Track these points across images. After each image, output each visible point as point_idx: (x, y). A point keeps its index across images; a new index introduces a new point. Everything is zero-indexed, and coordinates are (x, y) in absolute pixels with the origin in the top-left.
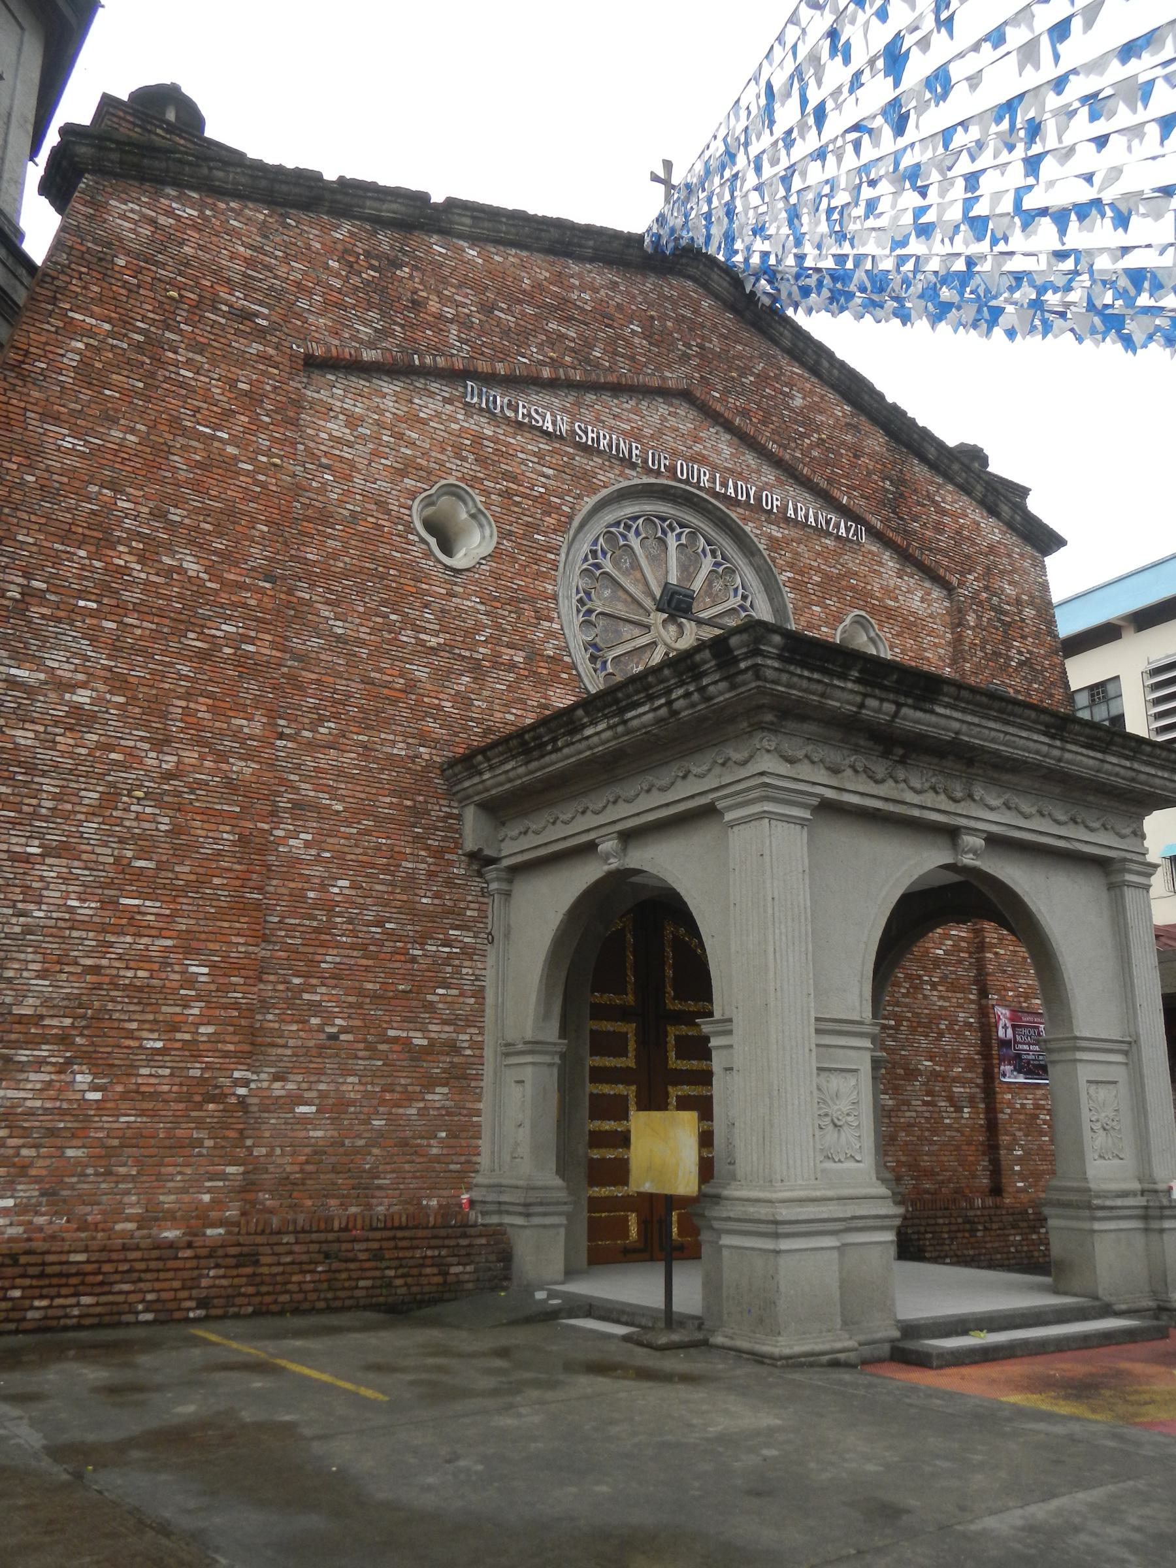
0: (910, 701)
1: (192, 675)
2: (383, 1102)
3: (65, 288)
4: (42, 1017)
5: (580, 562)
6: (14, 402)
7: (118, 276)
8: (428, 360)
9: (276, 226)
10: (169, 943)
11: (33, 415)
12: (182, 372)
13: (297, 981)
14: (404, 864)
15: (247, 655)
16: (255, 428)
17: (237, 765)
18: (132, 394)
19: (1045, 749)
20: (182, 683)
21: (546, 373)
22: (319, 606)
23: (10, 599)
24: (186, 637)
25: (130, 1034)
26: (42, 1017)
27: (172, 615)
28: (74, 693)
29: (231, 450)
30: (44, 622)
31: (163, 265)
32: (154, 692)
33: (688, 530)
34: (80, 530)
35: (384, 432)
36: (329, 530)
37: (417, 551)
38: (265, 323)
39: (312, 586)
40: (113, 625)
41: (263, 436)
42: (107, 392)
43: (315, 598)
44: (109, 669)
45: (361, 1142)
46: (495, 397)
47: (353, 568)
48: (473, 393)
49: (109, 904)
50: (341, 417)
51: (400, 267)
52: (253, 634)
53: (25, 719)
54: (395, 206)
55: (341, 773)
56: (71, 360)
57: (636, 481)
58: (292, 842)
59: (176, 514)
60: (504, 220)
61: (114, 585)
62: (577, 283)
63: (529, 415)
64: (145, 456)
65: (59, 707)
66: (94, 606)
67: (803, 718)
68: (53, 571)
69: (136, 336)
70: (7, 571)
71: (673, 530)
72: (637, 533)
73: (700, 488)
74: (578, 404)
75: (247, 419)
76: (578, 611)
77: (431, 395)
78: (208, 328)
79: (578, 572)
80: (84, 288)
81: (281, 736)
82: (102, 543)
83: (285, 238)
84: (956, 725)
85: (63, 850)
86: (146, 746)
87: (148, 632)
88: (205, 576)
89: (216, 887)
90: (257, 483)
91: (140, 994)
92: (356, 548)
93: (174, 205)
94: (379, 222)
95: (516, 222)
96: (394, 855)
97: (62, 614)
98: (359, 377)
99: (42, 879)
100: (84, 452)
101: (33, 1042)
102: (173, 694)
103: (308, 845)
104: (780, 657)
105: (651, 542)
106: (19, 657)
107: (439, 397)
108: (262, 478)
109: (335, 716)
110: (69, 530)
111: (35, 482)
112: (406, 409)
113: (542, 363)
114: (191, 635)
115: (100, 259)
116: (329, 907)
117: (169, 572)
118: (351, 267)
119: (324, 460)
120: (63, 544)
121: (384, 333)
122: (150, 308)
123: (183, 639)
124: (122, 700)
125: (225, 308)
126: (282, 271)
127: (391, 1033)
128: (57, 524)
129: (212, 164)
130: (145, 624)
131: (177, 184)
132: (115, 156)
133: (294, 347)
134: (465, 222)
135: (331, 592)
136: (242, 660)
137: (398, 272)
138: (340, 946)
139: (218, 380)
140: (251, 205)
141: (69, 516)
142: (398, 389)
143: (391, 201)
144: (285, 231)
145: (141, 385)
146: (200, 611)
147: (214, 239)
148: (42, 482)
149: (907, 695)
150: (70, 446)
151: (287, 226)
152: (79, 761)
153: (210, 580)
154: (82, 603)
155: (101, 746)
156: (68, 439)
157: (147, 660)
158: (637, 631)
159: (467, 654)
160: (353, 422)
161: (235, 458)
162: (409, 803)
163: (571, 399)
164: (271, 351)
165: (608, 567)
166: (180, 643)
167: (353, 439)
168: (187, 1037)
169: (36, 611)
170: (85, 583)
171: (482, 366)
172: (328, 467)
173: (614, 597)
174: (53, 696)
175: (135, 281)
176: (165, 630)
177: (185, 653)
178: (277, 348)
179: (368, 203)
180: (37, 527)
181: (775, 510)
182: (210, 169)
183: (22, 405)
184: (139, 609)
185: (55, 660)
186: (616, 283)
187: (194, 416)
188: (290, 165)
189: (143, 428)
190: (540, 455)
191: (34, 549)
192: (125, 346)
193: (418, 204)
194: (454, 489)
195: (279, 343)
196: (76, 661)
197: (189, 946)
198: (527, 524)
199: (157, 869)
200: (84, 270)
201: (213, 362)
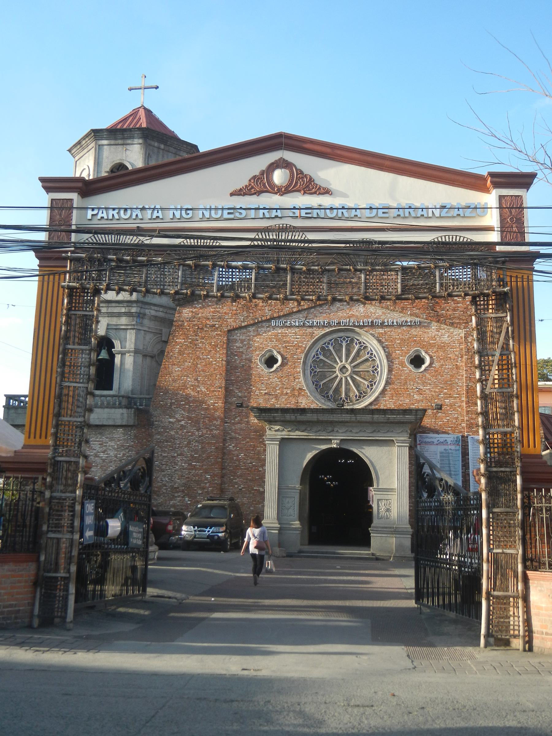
0: (299, 415)
2: (253, 504)
4: (179, 487)
5: (311, 359)
8: (260, 319)
10: (202, 471)
13: (232, 477)
14: (258, 449)
17: (215, 432)
19: (349, 417)
21: (295, 310)
25: (195, 490)
26: (179, 487)
29: (211, 360)
33: (350, 338)
37: (259, 370)
39: (233, 385)
40: (187, 406)
44: (188, 416)
45: (248, 513)
46: (280, 322)
48: (273, 323)
49: (190, 464)
53: (172, 429)
55: (241, 429)
56: (177, 351)
57: (328, 330)
58: (230, 447)
63: (291, 323)
67: (276, 421)
71: (344, 339)
72: (332, 344)
73: (350, 326)
74: (308, 314)
76: (311, 373)
77: (263, 327)
79: (311, 361)
81: (227, 423)
84: (316, 417)
85: (181, 454)
86: (195, 431)
89: (211, 459)
91: (198, 482)
96: (254, 446)
99: (177, 460)
101: (177, 492)
103: (233, 447)
104: (258, 413)
105: (338, 345)
106: (171, 417)
109: (239, 416)
116: (239, 460)
117: (198, 392)
119: (235, 354)
124: (190, 422)
127: (255, 488)
131: (196, 300)
138: (242, 469)
147: (205, 310)
149: (297, 414)
152: (183, 436)
155: (187, 432)
158: (331, 374)
159: (273, 393)
160: (242, 343)
161: (212, 362)
162: (258, 434)
163: (306, 313)
164: (219, 332)
165: (322, 357)
168: (206, 490)
171: (275, 315)
172: (236, 355)
173: (324, 365)
174: (177, 423)
181: (379, 325)
185: (178, 416)
189: (191, 361)
190: (296, 334)
197: (206, 472)
198: (292, 354)
199: (199, 456)
201: (206, 340)
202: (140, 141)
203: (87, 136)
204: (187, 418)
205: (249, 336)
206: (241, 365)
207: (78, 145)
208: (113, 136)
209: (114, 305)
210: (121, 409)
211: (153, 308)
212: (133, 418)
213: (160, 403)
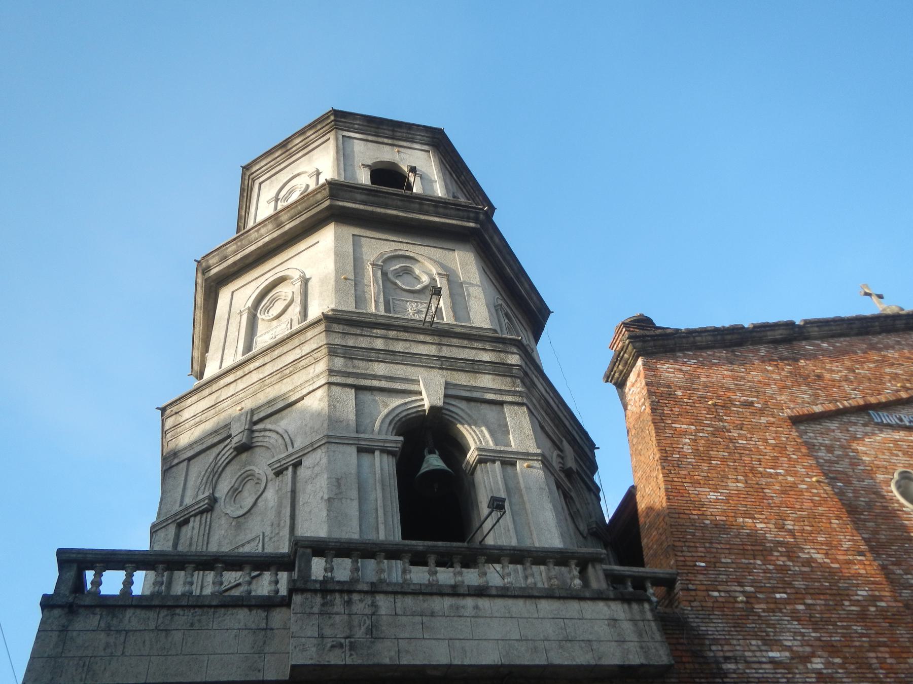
1: (864, 632)
3: (663, 413)
6: (675, 479)
7: (682, 400)
9: (733, 357)
11: (688, 485)
12: (740, 441)
15: (882, 610)
16: (792, 463)
18: (725, 460)
20: (864, 639)
21: (904, 395)
22: (891, 567)
23: (742, 602)
24: (843, 605)
27: (828, 591)
28: (811, 662)
29: (790, 479)
30: (766, 614)
31: (698, 390)
32: (853, 650)
34: (749, 548)
35: (848, 450)
36: (862, 517)
38: (759, 406)
40: (801, 607)
41: (800, 466)
42: (713, 462)
43: (886, 562)
44: (818, 639)
47: (891, 537)
50: (822, 448)
51: (798, 360)
52: (877, 593)
54: (780, 332)
56: (687, 449)
59: (789, 525)
60: (832, 323)
61: (786, 579)
62: (882, 346)
64: (753, 493)
65: (809, 675)
66: (785, 596)
68: (751, 577)
69: (708, 429)
70: (729, 584)
75: (786, 459)
77: (855, 424)
78: (737, 415)
80: (671, 410)
82: (765, 553)
83: (741, 361)
87: (823, 607)
88: (827, 561)
90: (815, 495)
92: (883, 524)
93: (685, 360)
94: (776, 342)
95: (839, 323)
97: (772, 606)
98: (815, 424)
100: (723, 499)
102: (864, 650)
106: (771, 643)
107: (859, 424)
108: (815, 491)
110: (744, 549)
111: (711, 524)
112: (848, 435)
113: (897, 391)
114: (847, 603)
115: (670, 394)
118: (777, 367)
119: (831, 475)
120: (745, 559)
121: (816, 396)
122: (705, 412)
123: (844, 607)
125: (737, 403)
126: (749, 378)
128: (735, 547)
129: (694, 334)
130: (819, 602)
131: (682, 350)
132: (652, 344)
133: (781, 414)
134: (814, 331)
135: (890, 556)
136: (884, 613)
137: (800, 364)
139: (759, 441)
140: (716, 351)
141: (739, 540)
142: (837, 425)
143: (778, 329)
144: (738, 359)
145: (726, 454)
146: (840, 585)
147: (711, 371)
148: (714, 522)
150: (715, 497)
151: (737, 356)
153: (832, 563)
154: (778, 596)
156: (711, 494)
157: (836, 627)
160: (830, 449)
164: (772, 420)
166: (844, 610)
167: (836, 459)
169: (759, 607)
170: (771, 581)
171: (873, 400)
174: (801, 667)
175: (690, 401)
176: (831, 603)
177: (851, 616)
178: (773, 417)
179: (769, 333)
180: (727, 551)
182: (694, 337)
183: (680, 480)
184: (808, 592)
186: (898, 341)
187: (760, 464)
188: (727, 325)
191: (734, 566)
192: (707, 435)
193: (791, 327)
194: (905, 474)
195: (772, 414)
196: (799, 638)
200: (666, 402)
202: (426, 148)
203: (312, 126)
204: (823, 648)
205: (839, 440)
206: (863, 503)
207: (277, 150)
208: (373, 129)
209: (455, 341)
210: (601, 605)
211: (541, 380)
212: (658, 636)
213: (709, 595)
